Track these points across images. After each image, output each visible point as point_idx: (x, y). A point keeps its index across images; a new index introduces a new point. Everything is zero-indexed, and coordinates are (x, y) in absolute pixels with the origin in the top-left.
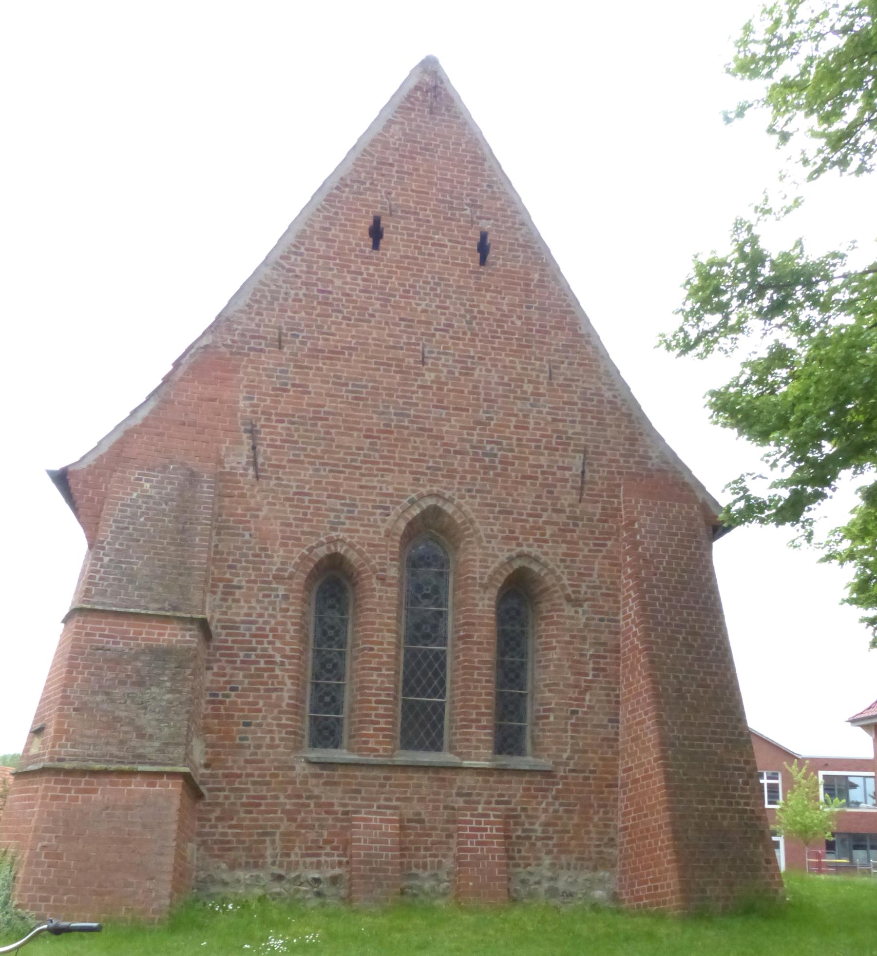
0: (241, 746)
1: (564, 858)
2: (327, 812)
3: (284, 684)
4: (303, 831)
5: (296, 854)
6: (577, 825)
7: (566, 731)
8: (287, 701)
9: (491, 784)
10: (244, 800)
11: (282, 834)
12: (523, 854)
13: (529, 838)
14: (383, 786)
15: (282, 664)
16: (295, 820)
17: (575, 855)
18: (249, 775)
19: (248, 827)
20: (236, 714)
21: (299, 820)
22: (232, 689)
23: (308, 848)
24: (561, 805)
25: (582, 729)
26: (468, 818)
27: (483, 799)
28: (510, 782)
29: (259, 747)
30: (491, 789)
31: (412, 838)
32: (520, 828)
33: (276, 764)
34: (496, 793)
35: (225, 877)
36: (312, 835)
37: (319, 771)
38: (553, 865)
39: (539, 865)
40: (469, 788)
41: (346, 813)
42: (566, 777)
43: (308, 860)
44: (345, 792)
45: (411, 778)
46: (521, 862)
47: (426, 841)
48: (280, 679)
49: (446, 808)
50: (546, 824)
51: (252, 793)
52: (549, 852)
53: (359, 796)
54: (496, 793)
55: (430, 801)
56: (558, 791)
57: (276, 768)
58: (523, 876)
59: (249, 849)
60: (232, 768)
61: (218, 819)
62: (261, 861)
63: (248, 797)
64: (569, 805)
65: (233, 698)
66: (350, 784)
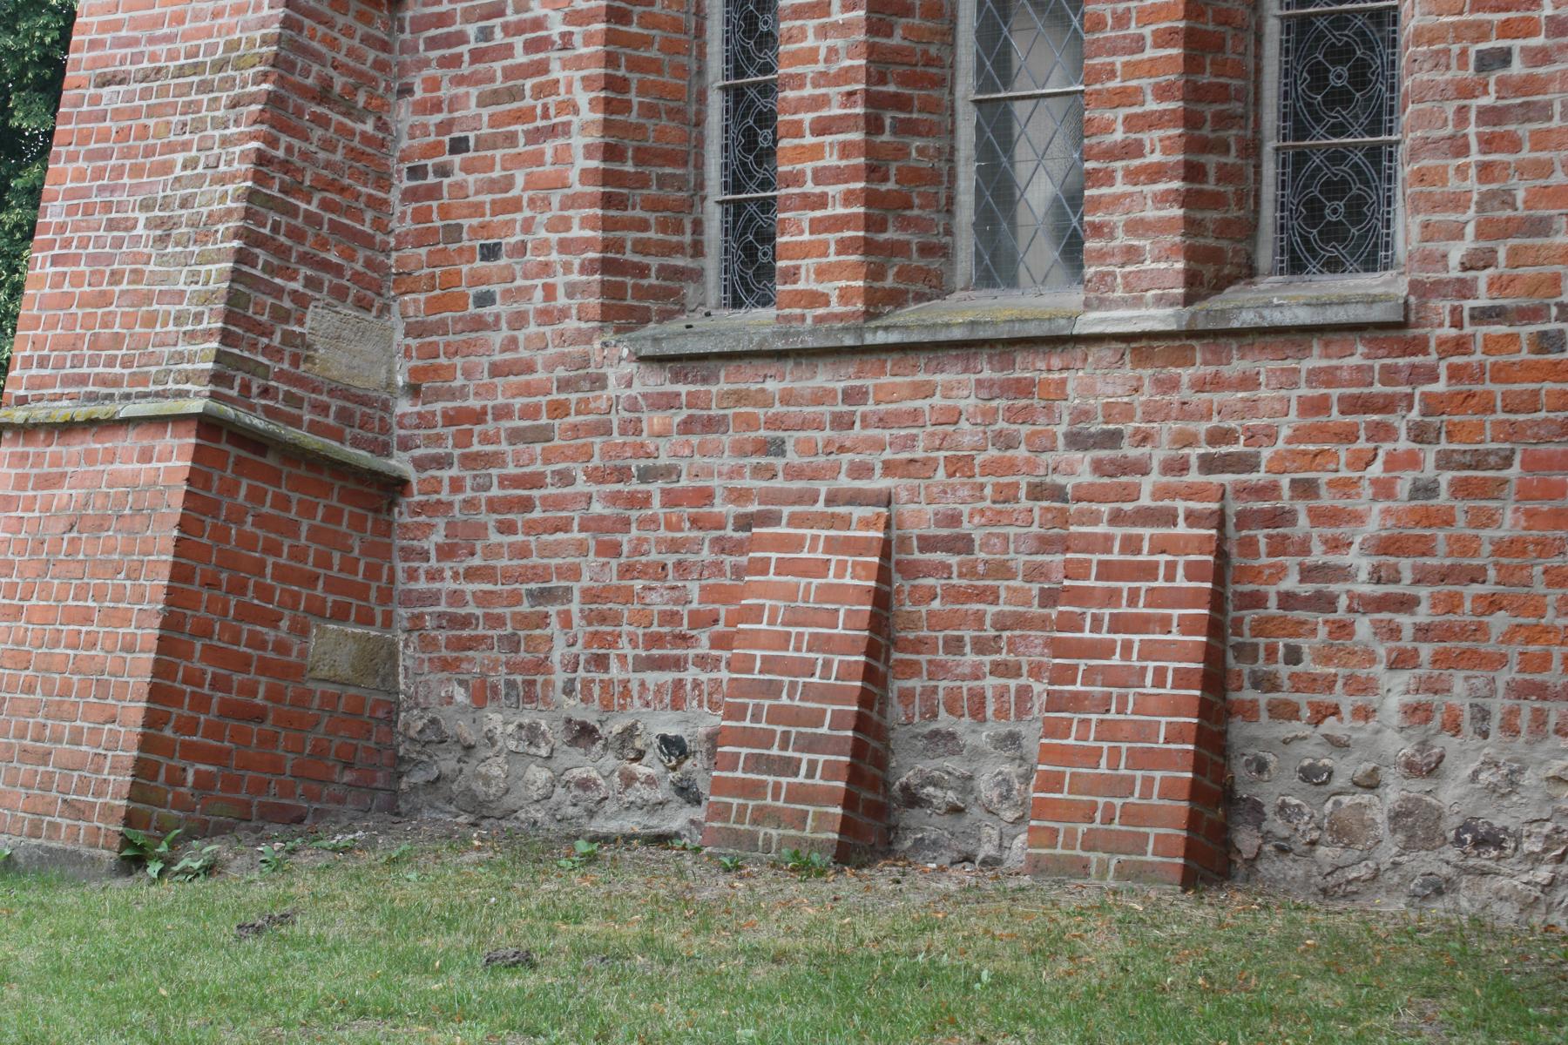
0: (479, 324)
1: (1460, 689)
2: (695, 522)
3: (571, 107)
4: (638, 585)
5: (622, 659)
6: (1503, 548)
7: (1463, 150)
8: (581, 163)
9: (1185, 393)
10: (495, 491)
11: (590, 596)
12: (1308, 666)
13: (1325, 602)
14: (842, 422)
15: (567, 42)
16: (613, 550)
17: (1504, 676)
18: (503, 413)
19: (508, 576)
20: (466, 222)
21: (625, 549)
22: (459, 146)
23: (654, 640)
24: (1445, 461)
25: (1524, 130)
26: (1102, 528)
27: (1158, 454)
28: (1248, 382)
29: (519, 320)
30: (1185, 412)
31: (936, 605)
32: (1291, 562)
33: (560, 372)
34: (1203, 427)
35: (463, 728)
36: (658, 601)
37: (670, 388)
38: (1417, 713)
39: (1364, 713)
40: (1109, 412)
41: (745, 522)
42: (1460, 345)
43: (653, 678)
44: (740, 450)
45: (926, 391)
46: (1301, 699)
47: (979, 618)
48: (563, 96)
49: (1036, 492)
50: (1386, 546)
51: (511, 470)
52: (1400, 661)
53: (779, 462)
54: (1203, 427)
55: (990, 468)
56: (1433, 405)
57: (564, 385)
58: (1312, 752)
59: (513, 643)
60: (462, 393)
61: (446, 552)
62: (540, 679)
63: (504, 481)
64: (1479, 461)
65: (458, 176)
66: (749, 423)
